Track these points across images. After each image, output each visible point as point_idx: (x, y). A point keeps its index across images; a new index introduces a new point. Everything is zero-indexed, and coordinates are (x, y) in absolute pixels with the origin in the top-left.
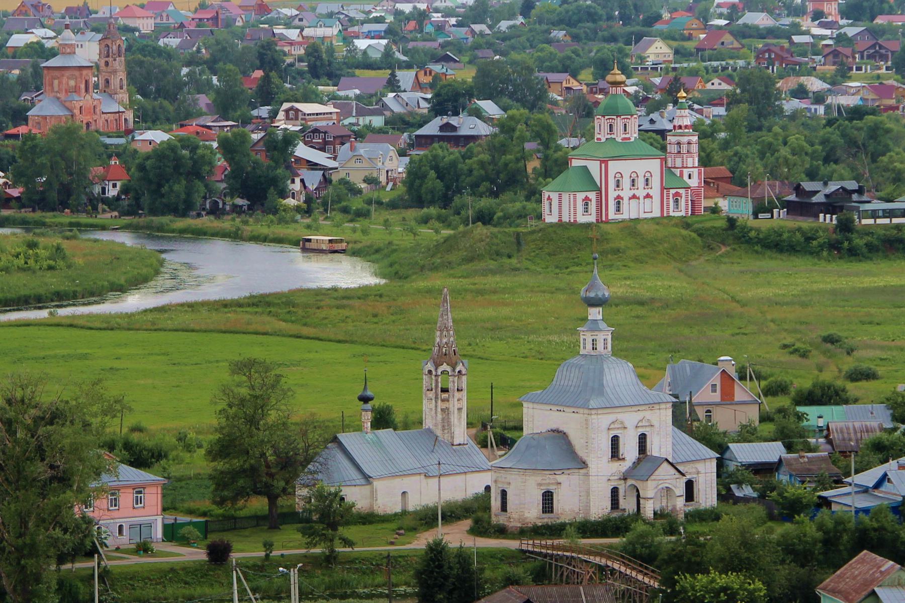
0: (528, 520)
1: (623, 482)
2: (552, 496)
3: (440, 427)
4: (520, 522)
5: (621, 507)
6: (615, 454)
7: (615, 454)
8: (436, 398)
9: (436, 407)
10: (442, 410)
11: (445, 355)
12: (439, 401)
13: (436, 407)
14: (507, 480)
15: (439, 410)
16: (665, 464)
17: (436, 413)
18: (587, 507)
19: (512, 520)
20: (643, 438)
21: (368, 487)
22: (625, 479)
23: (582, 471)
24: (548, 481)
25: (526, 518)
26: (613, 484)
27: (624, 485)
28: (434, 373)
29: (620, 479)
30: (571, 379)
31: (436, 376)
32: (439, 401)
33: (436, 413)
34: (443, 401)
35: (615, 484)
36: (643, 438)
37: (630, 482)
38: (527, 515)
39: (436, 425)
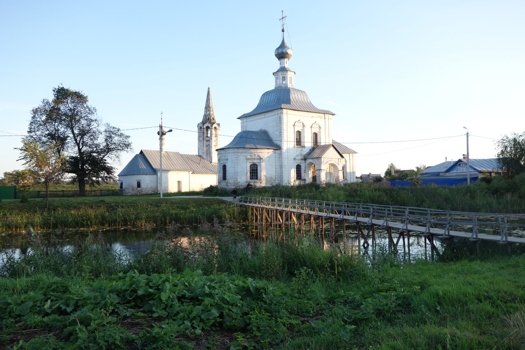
0: (240, 184)
1: (304, 161)
2: (257, 168)
3: (205, 154)
4: (234, 185)
5: (302, 178)
6: (299, 142)
7: (299, 142)
8: (203, 140)
9: (203, 144)
10: (206, 146)
11: (209, 119)
12: (205, 141)
13: (203, 144)
14: (226, 158)
15: (205, 145)
16: (332, 148)
17: (203, 147)
18: (281, 177)
19: (229, 184)
20: (316, 135)
21: (155, 176)
22: (305, 159)
23: (277, 152)
24: (253, 157)
25: (239, 182)
26: (297, 162)
27: (304, 164)
28: (202, 128)
29: (302, 159)
30: (269, 99)
31: (203, 129)
32: (205, 141)
33: (203, 147)
34: (207, 141)
35: (298, 162)
36: (316, 135)
37: (308, 161)
38: (239, 180)
39: (203, 153)
